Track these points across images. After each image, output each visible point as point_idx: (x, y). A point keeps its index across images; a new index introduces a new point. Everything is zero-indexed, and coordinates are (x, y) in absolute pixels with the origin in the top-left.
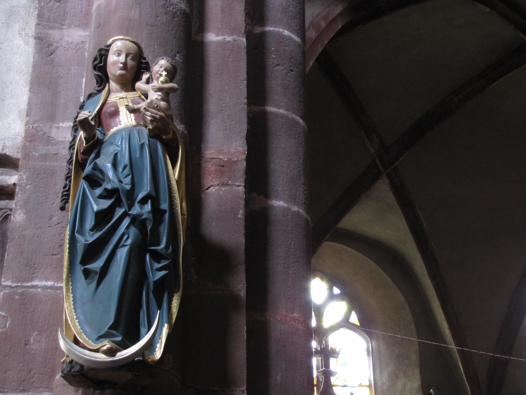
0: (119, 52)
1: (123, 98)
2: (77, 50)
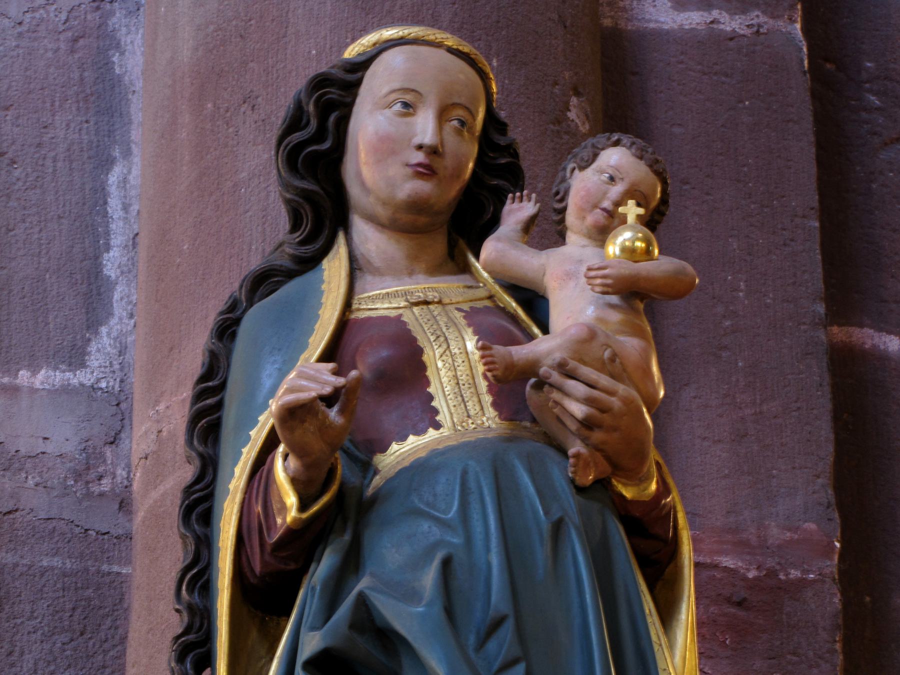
0: (408, 98)
1: (426, 303)
2: (75, 40)
